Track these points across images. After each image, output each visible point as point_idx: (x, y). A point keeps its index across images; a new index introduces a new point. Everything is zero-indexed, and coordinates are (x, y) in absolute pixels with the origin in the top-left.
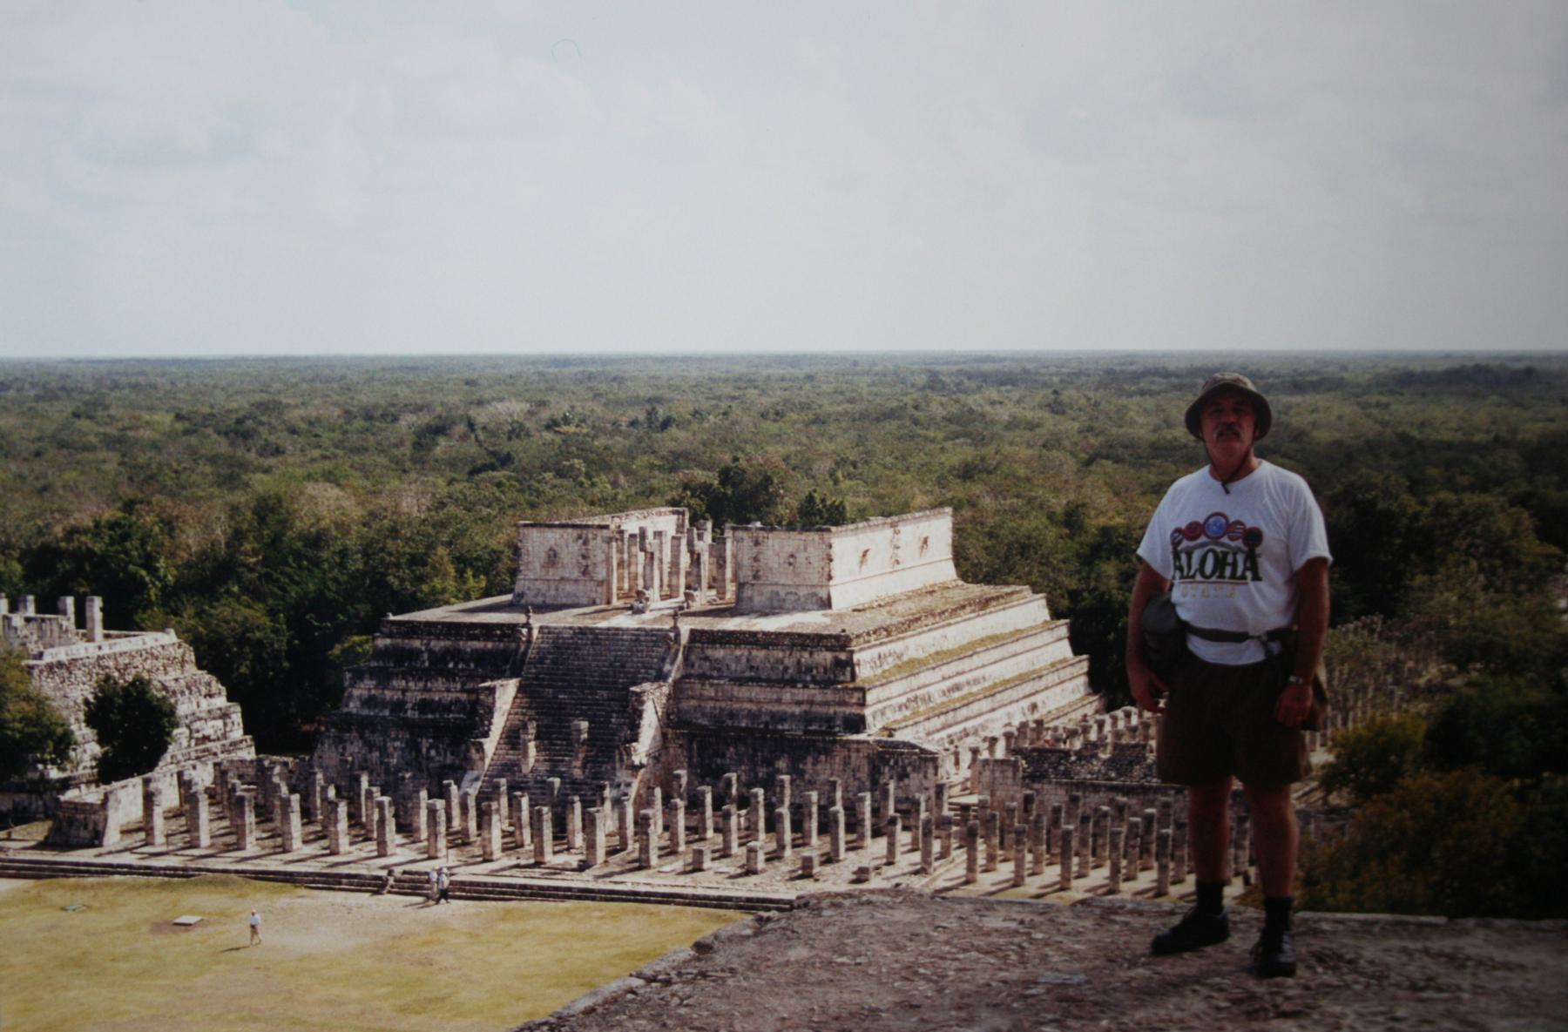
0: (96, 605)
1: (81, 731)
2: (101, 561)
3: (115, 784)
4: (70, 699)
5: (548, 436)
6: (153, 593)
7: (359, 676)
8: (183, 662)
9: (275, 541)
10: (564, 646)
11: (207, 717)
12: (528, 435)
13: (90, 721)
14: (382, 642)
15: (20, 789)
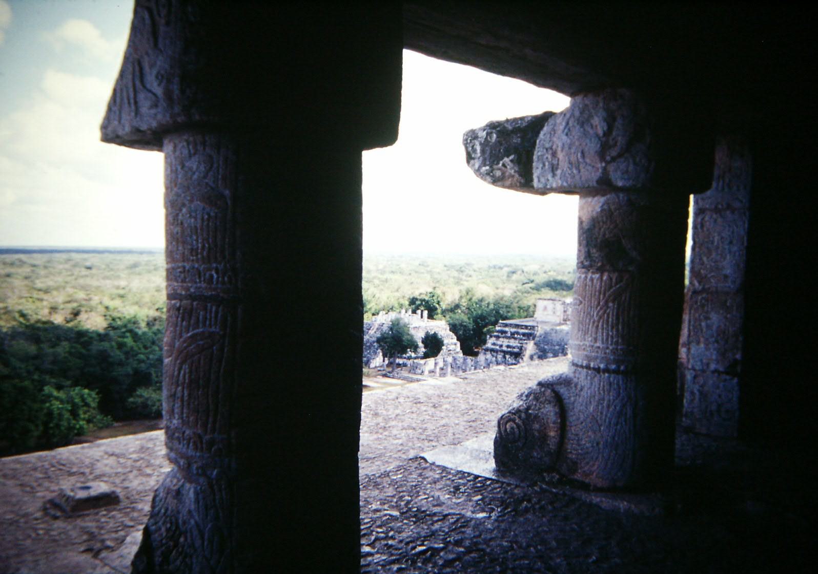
0: (426, 313)
1: (421, 345)
2: (427, 302)
3: (428, 359)
4: (419, 336)
5: (544, 275)
6: (439, 311)
7: (491, 337)
8: (446, 330)
9: (470, 300)
10: (546, 334)
11: (451, 342)
12: (539, 274)
13: (423, 342)
14: (498, 328)
15: (405, 358)
